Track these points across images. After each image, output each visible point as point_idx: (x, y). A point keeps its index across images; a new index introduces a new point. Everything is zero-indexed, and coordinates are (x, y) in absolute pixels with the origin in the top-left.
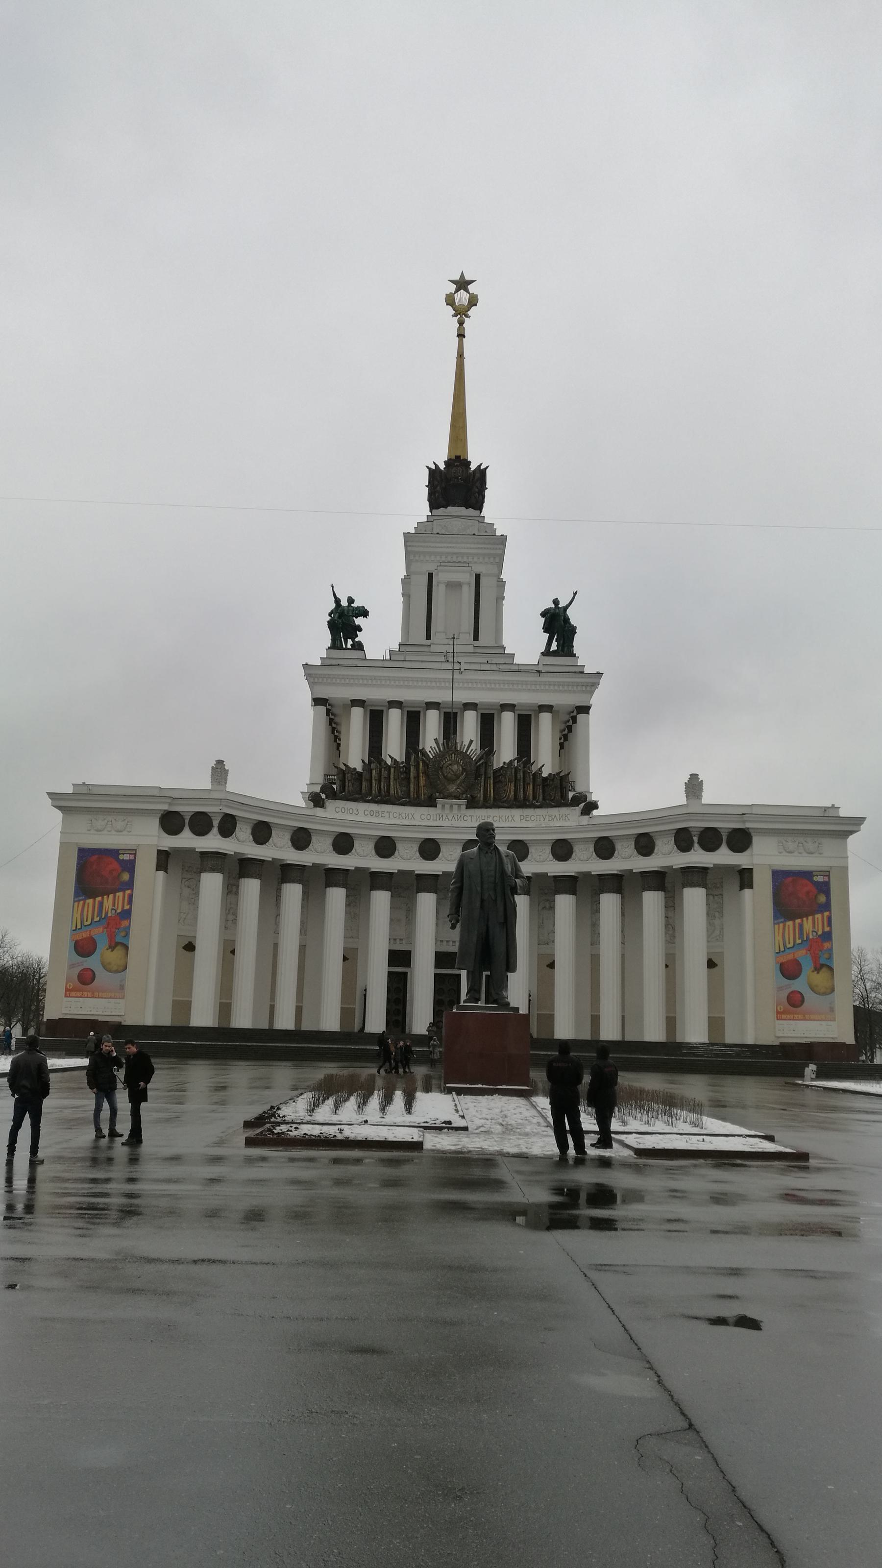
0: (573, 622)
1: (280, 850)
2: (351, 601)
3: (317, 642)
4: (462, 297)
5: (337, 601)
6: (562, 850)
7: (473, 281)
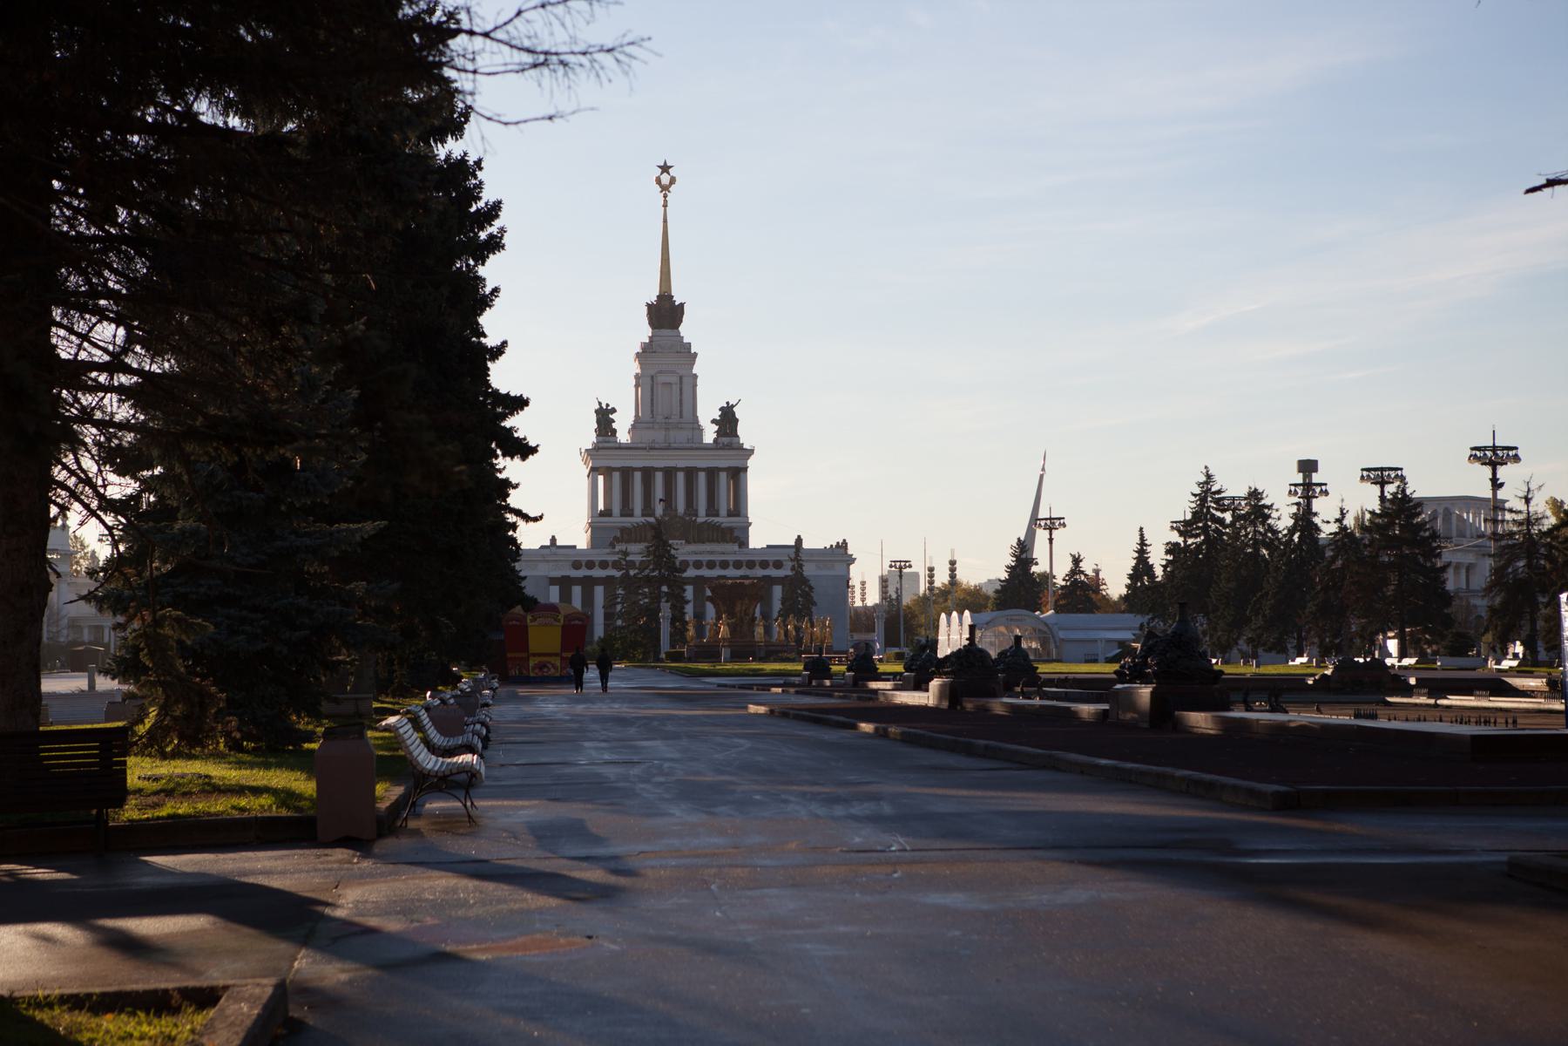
4: (665, 179)
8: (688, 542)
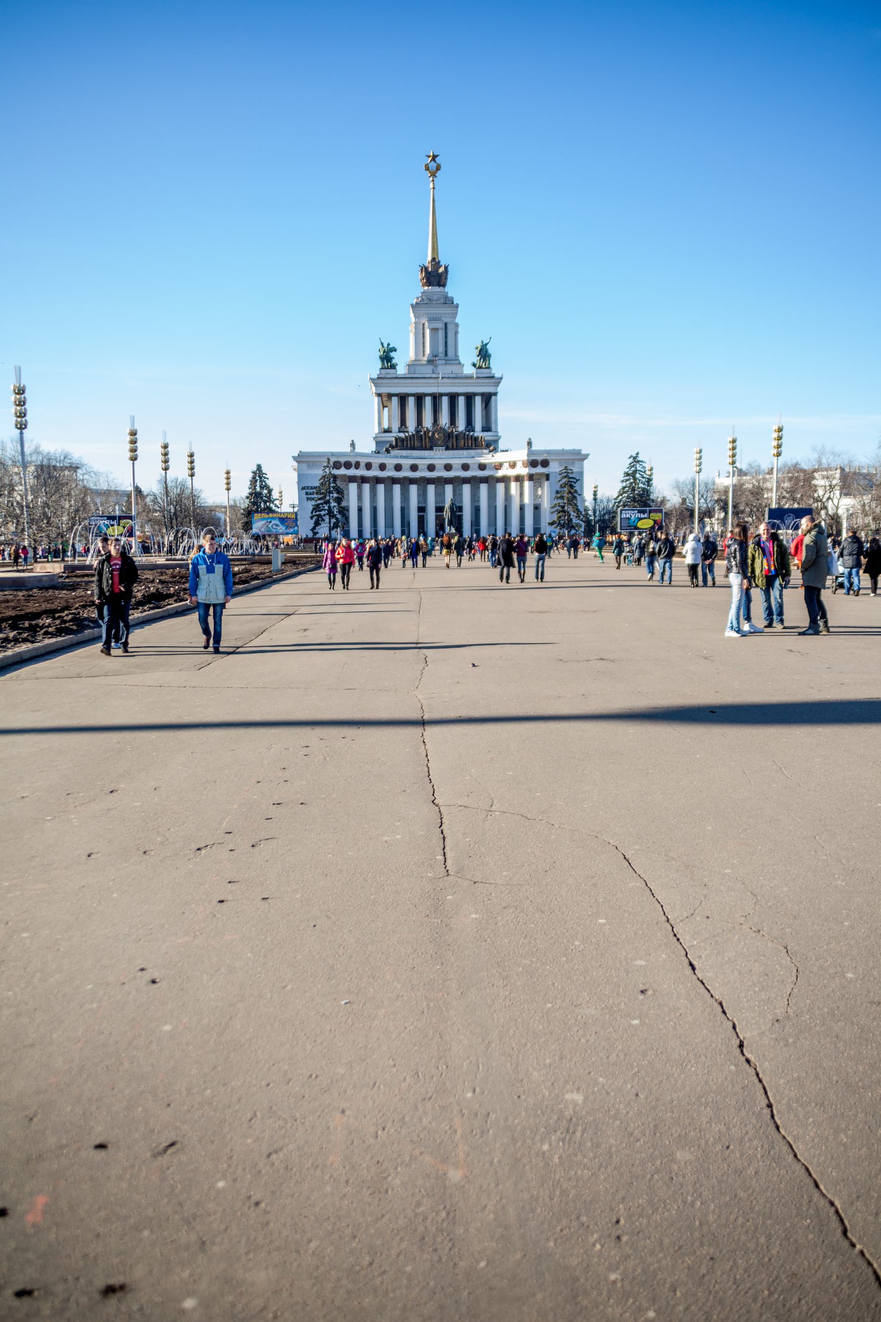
0: (490, 351)
1: (375, 473)
2: (389, 345)
3: (375, 368)
4: (433, 166)
5: (382, 344)
6: (482, 467)
7: (437, 156)
8: (447, 449)
